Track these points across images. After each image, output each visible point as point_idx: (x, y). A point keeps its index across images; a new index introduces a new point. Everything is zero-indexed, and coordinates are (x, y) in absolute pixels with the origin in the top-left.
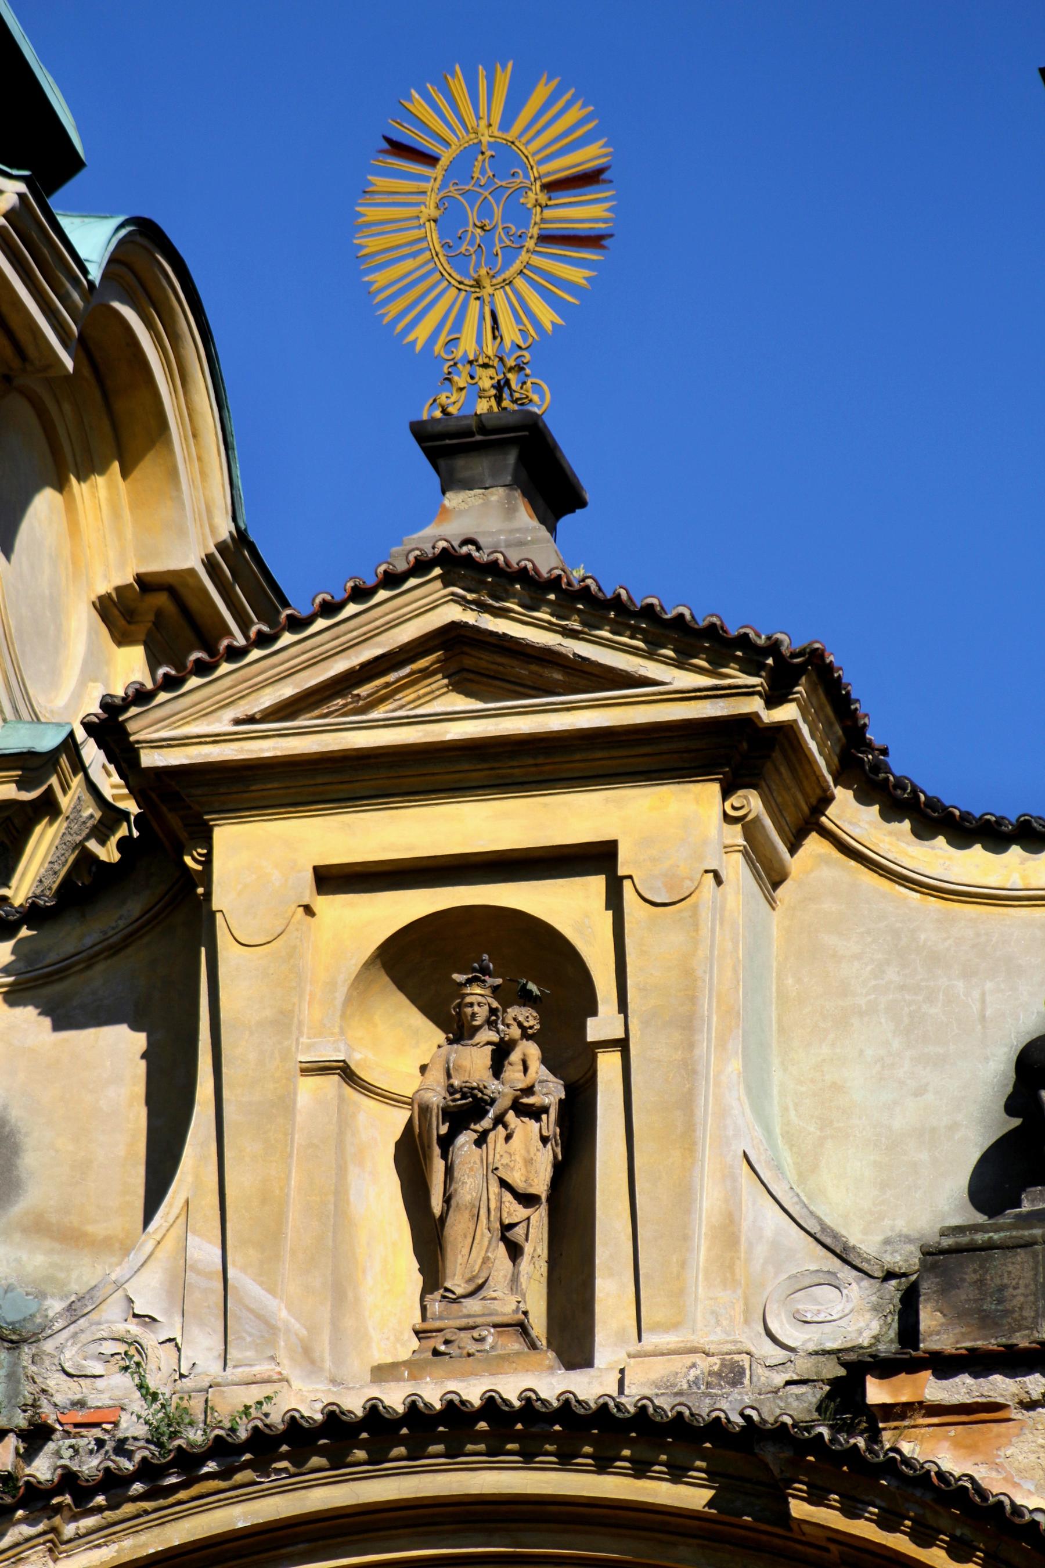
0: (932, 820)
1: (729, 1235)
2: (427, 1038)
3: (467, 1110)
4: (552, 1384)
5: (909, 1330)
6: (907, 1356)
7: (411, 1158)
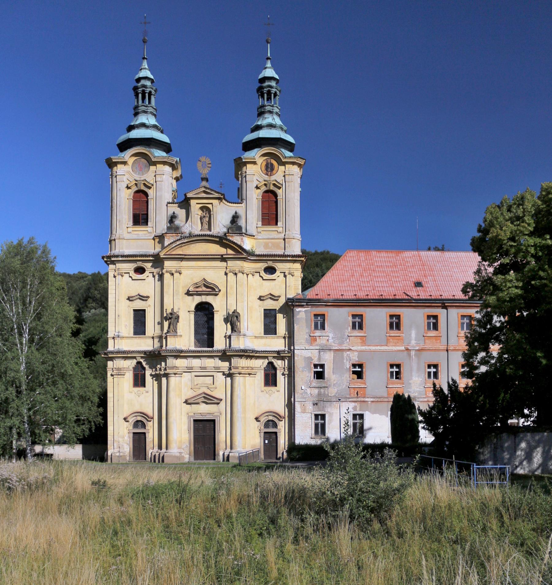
0: (228, 202)
1: (219, 225)
2: (202, 212)
3: (204, 217)
4: (208, 233)
5: (228, 231)
6: (228, 233)
7: (201, 219)
